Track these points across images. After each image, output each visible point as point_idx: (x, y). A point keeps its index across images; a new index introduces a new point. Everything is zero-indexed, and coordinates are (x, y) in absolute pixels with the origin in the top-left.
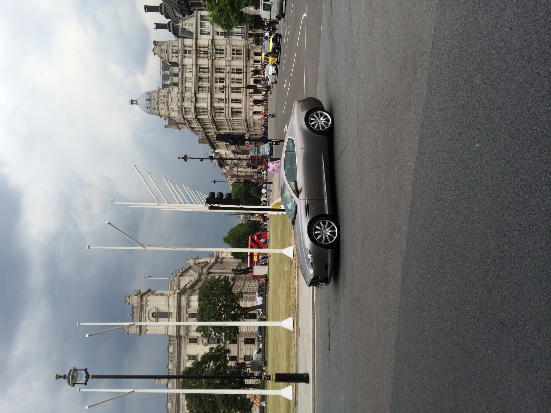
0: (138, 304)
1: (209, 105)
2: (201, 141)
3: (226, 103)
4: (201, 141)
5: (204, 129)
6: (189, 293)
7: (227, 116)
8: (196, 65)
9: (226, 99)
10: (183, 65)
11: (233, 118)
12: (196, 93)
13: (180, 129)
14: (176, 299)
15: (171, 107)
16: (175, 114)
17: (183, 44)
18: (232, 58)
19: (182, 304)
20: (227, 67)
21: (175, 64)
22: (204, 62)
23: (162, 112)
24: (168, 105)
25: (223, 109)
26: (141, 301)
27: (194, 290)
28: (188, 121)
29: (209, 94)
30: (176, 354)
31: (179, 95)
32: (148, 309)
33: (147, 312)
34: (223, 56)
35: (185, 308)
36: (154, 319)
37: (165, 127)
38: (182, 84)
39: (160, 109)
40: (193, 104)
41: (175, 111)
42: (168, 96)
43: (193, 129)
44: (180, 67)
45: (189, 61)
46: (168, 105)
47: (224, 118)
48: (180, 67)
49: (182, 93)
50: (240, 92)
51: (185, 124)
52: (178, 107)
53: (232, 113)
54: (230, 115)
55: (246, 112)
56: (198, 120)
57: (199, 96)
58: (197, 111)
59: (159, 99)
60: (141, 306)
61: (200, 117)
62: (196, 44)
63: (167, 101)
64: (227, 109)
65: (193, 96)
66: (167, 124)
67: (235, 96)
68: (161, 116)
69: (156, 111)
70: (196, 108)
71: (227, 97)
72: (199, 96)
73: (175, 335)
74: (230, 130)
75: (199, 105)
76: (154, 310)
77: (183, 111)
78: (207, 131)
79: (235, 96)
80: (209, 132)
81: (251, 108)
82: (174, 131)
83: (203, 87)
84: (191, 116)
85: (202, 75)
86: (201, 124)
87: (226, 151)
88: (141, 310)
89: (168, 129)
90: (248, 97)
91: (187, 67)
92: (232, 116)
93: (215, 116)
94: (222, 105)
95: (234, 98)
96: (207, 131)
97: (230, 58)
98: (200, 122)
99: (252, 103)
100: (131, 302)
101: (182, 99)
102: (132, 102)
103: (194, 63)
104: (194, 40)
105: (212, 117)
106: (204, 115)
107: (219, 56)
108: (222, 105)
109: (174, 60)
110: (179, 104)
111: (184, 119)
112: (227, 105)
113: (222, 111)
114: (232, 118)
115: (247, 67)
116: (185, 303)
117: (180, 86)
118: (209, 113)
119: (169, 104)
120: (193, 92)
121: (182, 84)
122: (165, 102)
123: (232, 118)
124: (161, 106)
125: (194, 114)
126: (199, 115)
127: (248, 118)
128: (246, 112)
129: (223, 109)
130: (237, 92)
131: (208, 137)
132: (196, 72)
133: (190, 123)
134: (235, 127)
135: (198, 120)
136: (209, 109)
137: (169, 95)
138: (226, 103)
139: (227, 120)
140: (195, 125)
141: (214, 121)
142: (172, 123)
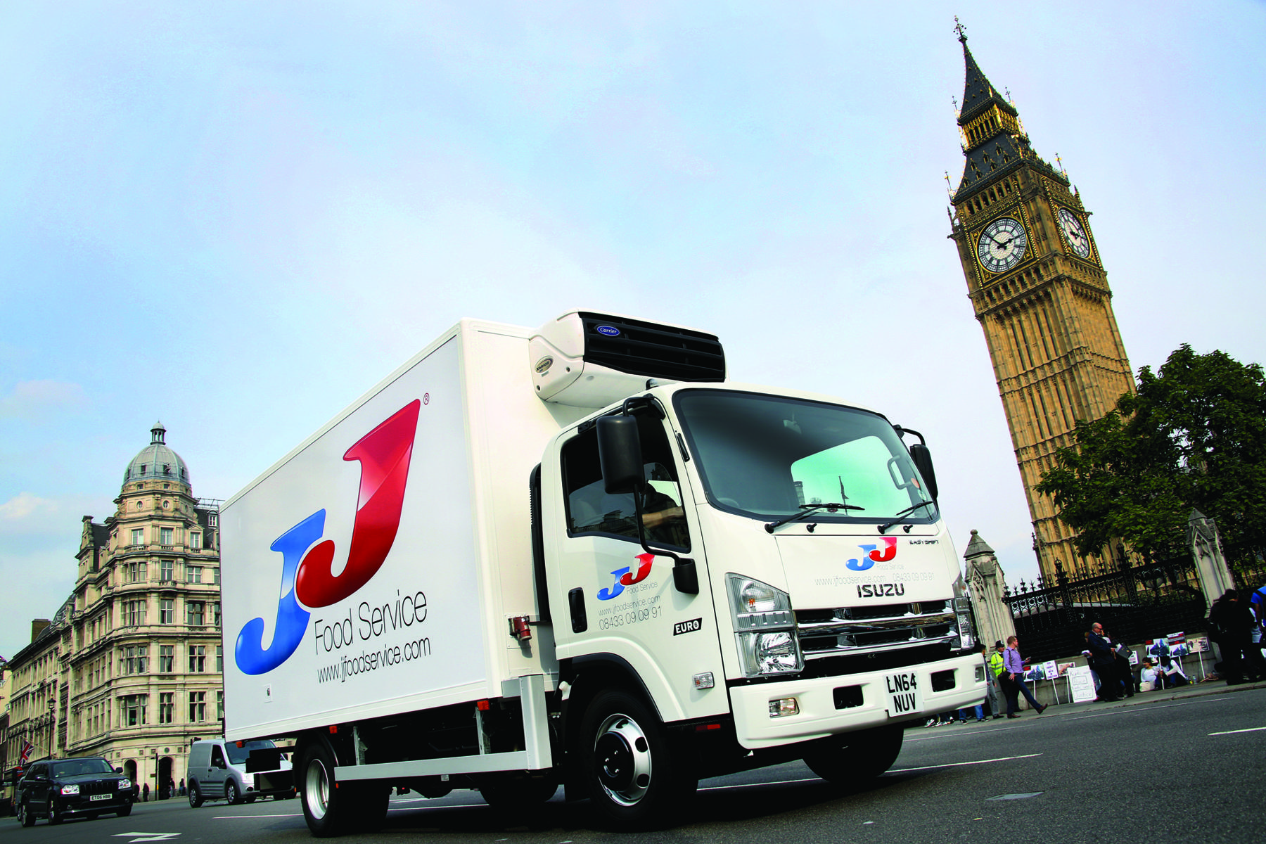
2: (38, 625)
3: (161, 677)
4: (38, 625)
5: (79, 624)
7: (121, 683)
9: (173, 677)
11: (114, 702)
12: (187, 593)
13: (79, 557)
15: (148, 526)
16: (124, 537)
23: (131, 503)
24: (151, 518)
25: (141, 670)
28: (106, 574)
29: (187, 630)
31: (179, 549)
37: (86, 518)
39: (140, 498)
40: (157, 585)
41: (136, 538)
42: (175, 519)
43: (80, 591)
46: (151, 518)
47: (115, 675)
49: (187, 559)
50: (192, 717)
51: (95, 568)
52: (145, 546)
53: (131, 698)
54: (123, 693)
55: (133, 737)
56: (108, 602)
57: (180, 601)
58: (133, 598)
59: (167, 498)
61: (117, 606)
63: (163, 518)
64: (144, 681)
65: (180, 586)
66: (93, 521)
67: (181, 701)
68: (119, 501)
69: (135, 489)
70: (144, 594)
71: (179, 680)
72: (180, 601)
74: (76, 698)
77: (133, 560)
78: (74, 633)
79: (181, 701)
80: (68, 639)
81: (148, 752)
82: (76, 538)
83: (202, 614)
84: (120, 580)
86: (94, 612)
87: (8, 699)
89: (81, 527)
90: (181, 739)
92: (120, 698)
93: (121, 648)
94: (154, 667)
95: (174, 699)
96: (74, 633)
98: (101, 608)
99: (161, 752)
101: (167, 557)
102: (159, 431)
105: (119, 639)
106: (124, 617)
108: (154, 667)
111: (112, 565)
112: (154, 680)
113: (136, 669)
114: (113, 697)
117: (203, 552)
118: (130, 631)
119: (155, 522)
120: (190, 587)
122: (160, 513)
123: (113, 697)
124: (149, 502)
125: (126, 588)
126: (124, 604)
127: (115, 745)
128: (133, 737)
129: (141, 670)
130: (192, 707)
131: (55, 637)
133: (101, 581)
134: (85, 712)
135: (108, 602)
136: (141, 630)
137: (181, 524)
138: (161, 677)
139: (109, 683)
140: (93, 596)
141: (103, 647)
142: (98, 535)
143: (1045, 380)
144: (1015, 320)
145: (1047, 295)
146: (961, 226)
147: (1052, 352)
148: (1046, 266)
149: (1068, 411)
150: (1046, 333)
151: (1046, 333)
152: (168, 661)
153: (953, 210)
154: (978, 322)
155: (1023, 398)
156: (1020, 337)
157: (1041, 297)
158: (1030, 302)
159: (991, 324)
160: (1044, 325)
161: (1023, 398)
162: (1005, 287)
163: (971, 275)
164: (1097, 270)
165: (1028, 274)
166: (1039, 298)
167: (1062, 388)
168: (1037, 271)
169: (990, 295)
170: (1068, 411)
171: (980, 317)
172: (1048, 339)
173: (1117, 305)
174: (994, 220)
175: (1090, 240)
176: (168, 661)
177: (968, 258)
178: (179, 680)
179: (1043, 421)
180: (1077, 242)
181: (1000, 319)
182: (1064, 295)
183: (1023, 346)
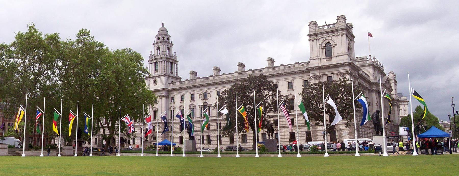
0: (338, 27)
6: (353, 74)
14: (345, 61)
19: (340, 69)
26: (341, 30)
27: (358, 79)
30: (293, 70)
32: (333, 38)
33: (330, 38)
35: (337, 72)
36: (324, 45)
60: (336, 31)
73: (310, 66)
76: (332, 43)
88: (331, 32)
100: (339, 21)
116: (342, 71)
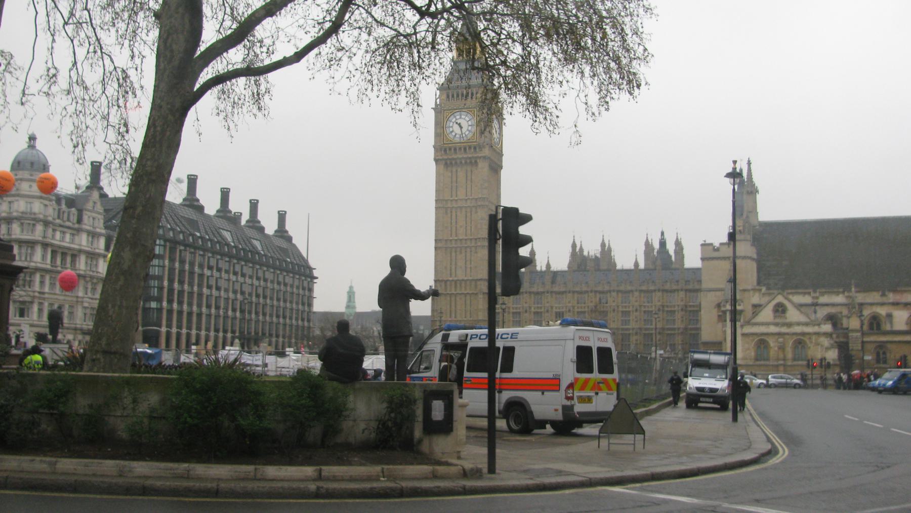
1: (39, 265)
3: (40, 293)
8: (80, 251)
9: (43, 293)
10: (79, 230)
17: (100, 235)
18: (85, 308)
20: (75, 299)
21: (80, 221)
22: (82, 264)
34: (90, 295)
38: (61, 226)
40: (40, 239)
44: (77, 226)
45: (83, 241)
48: (77, 226)
52: (35, 214)
53: (23, 303)
62: (99, 255)
71: (46, 296)
75: (39, 251)
85: (69, 259)
91: (76, 237)
94: (37, 287)
97: (86, 305)
101: (46, 223)
103: (83, 248)
104: (102, 252)
107: (90, 286)
108: (37, 287)
109: (85, 218)
110: (41, 216)
112: (37, 294)
115: (76, 329)
117: (58, 221)
121: (61, 226)
132: (73, 249)
136: (33, 264)
143: (461, 208)
144: (454, 170)
145: (476, 162)
146: (440, 104)
147: (469, 194)
148: (480, 148)
149: (469, 228)
150: (469, 182)
151: (469, 182)
152: (42, 283)
153: (438, 92)
154: (434, 163)
155: (446, 213)
156: (454, 179)
157: (473, 163)
158: (466, 163)
159: (442, 167)
160: (469, 178)
161: (446, 213)
162: (455, 149)
163: (437, 135)
164: (500, 155)
165: (470, 147)
166: (471, 162)
167: (469, 214)
168: (475, 148)
169: (445, 150)
170: (469, 228)
171: (436, 160)
172: (469, 186)
173: (503, 173)
174: (460, 110)
175: (501, 134)
176: (42, 283)
177: (440, 125)
178: (46, 296)
179: (454, 229)
180: (496, 136)
181: (446, 164)
182: (483, 166)
183: (454, 184)
